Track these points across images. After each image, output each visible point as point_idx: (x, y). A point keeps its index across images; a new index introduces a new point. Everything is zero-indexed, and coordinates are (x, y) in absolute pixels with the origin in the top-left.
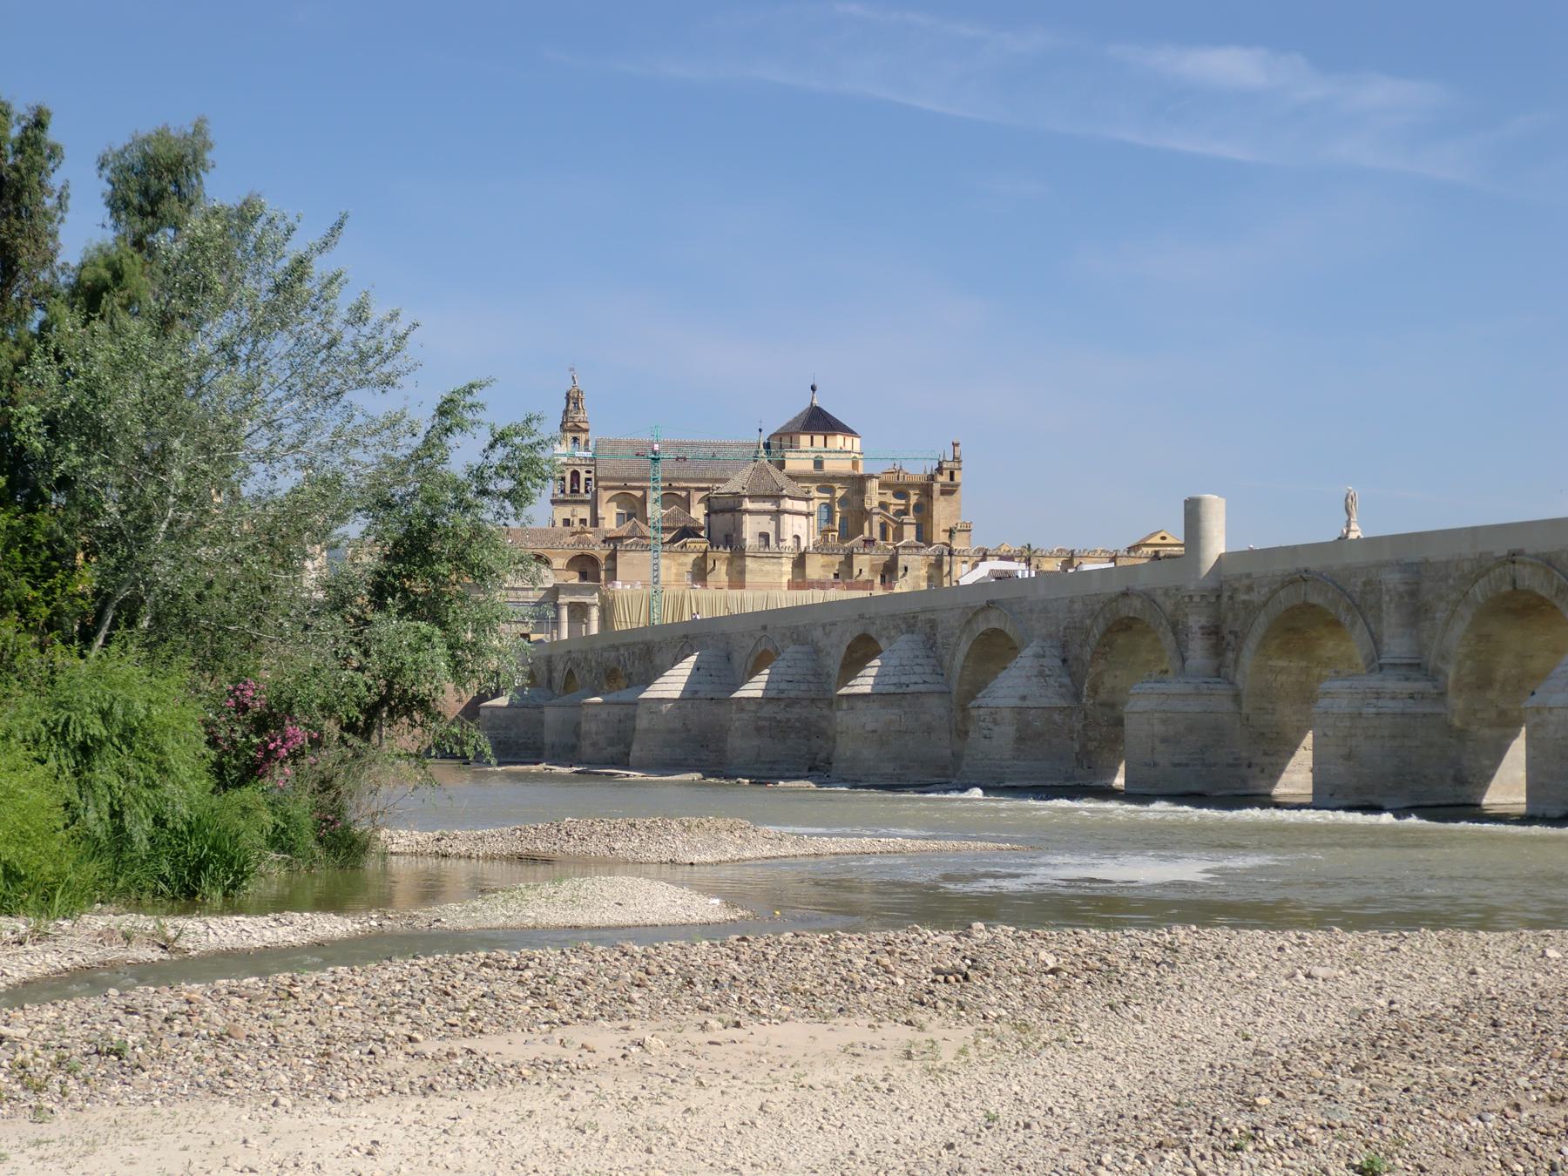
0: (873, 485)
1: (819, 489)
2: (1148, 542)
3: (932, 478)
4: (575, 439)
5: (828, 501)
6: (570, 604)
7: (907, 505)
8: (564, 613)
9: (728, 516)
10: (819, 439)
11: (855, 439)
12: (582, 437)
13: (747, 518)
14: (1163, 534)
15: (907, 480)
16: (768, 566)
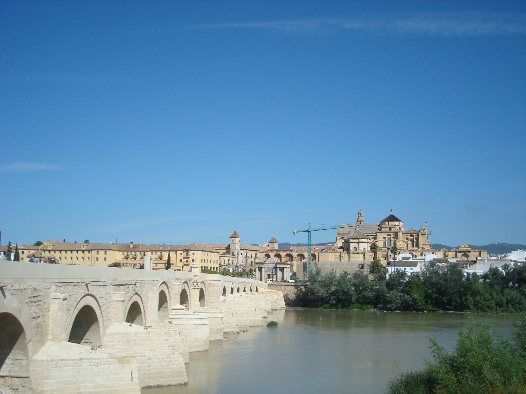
0: (400, 234)
1: (388, 235)
2: (460, 247)
3: (419, 231)
4: (360, 223)
5: (390, 238)
6: (280, 268)
7: (413, 239)
8: (278, 269)
9: (347, 243)
10: (390, 223)
11: (400, 222)
12: (362, 222)
13: (351, 244)
14: (465, 245)
15: (413, 232)
16: (356, 255)
